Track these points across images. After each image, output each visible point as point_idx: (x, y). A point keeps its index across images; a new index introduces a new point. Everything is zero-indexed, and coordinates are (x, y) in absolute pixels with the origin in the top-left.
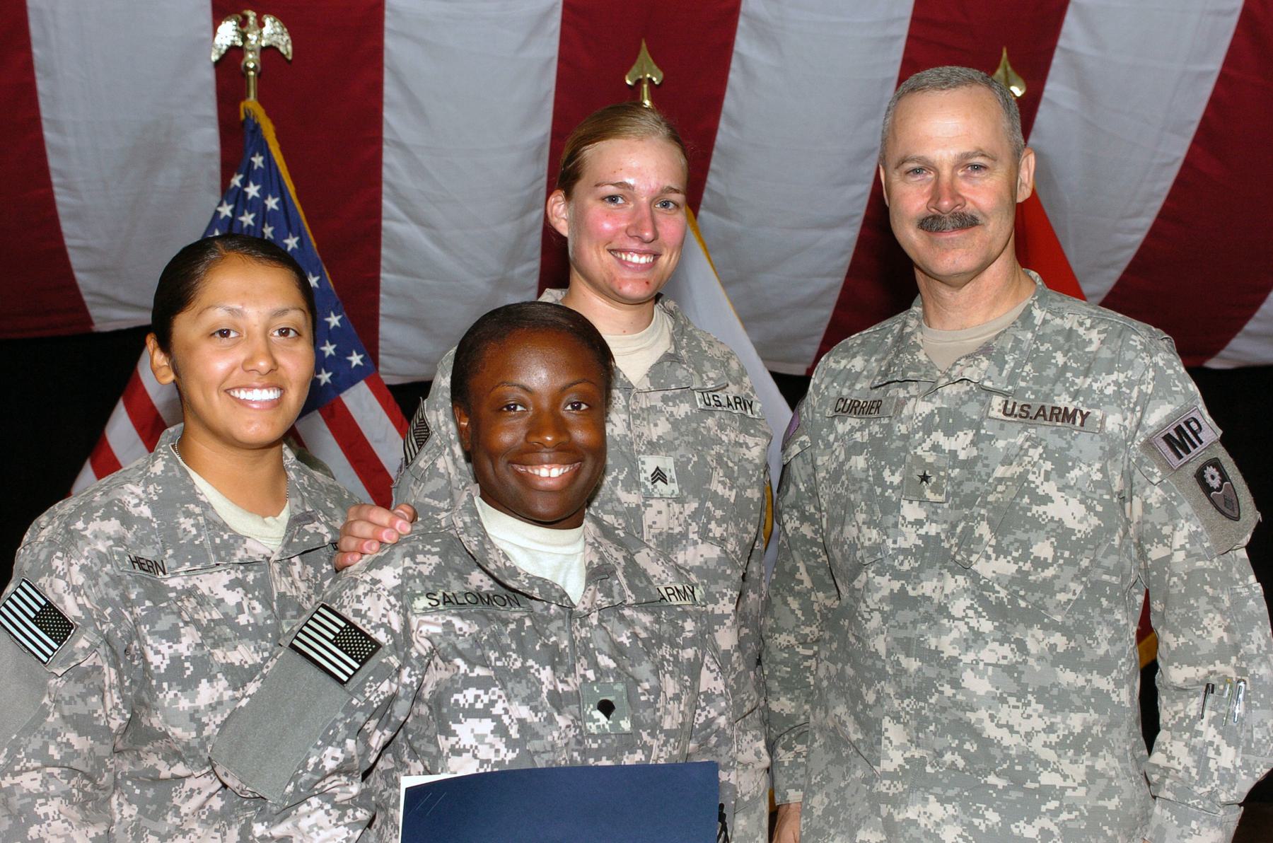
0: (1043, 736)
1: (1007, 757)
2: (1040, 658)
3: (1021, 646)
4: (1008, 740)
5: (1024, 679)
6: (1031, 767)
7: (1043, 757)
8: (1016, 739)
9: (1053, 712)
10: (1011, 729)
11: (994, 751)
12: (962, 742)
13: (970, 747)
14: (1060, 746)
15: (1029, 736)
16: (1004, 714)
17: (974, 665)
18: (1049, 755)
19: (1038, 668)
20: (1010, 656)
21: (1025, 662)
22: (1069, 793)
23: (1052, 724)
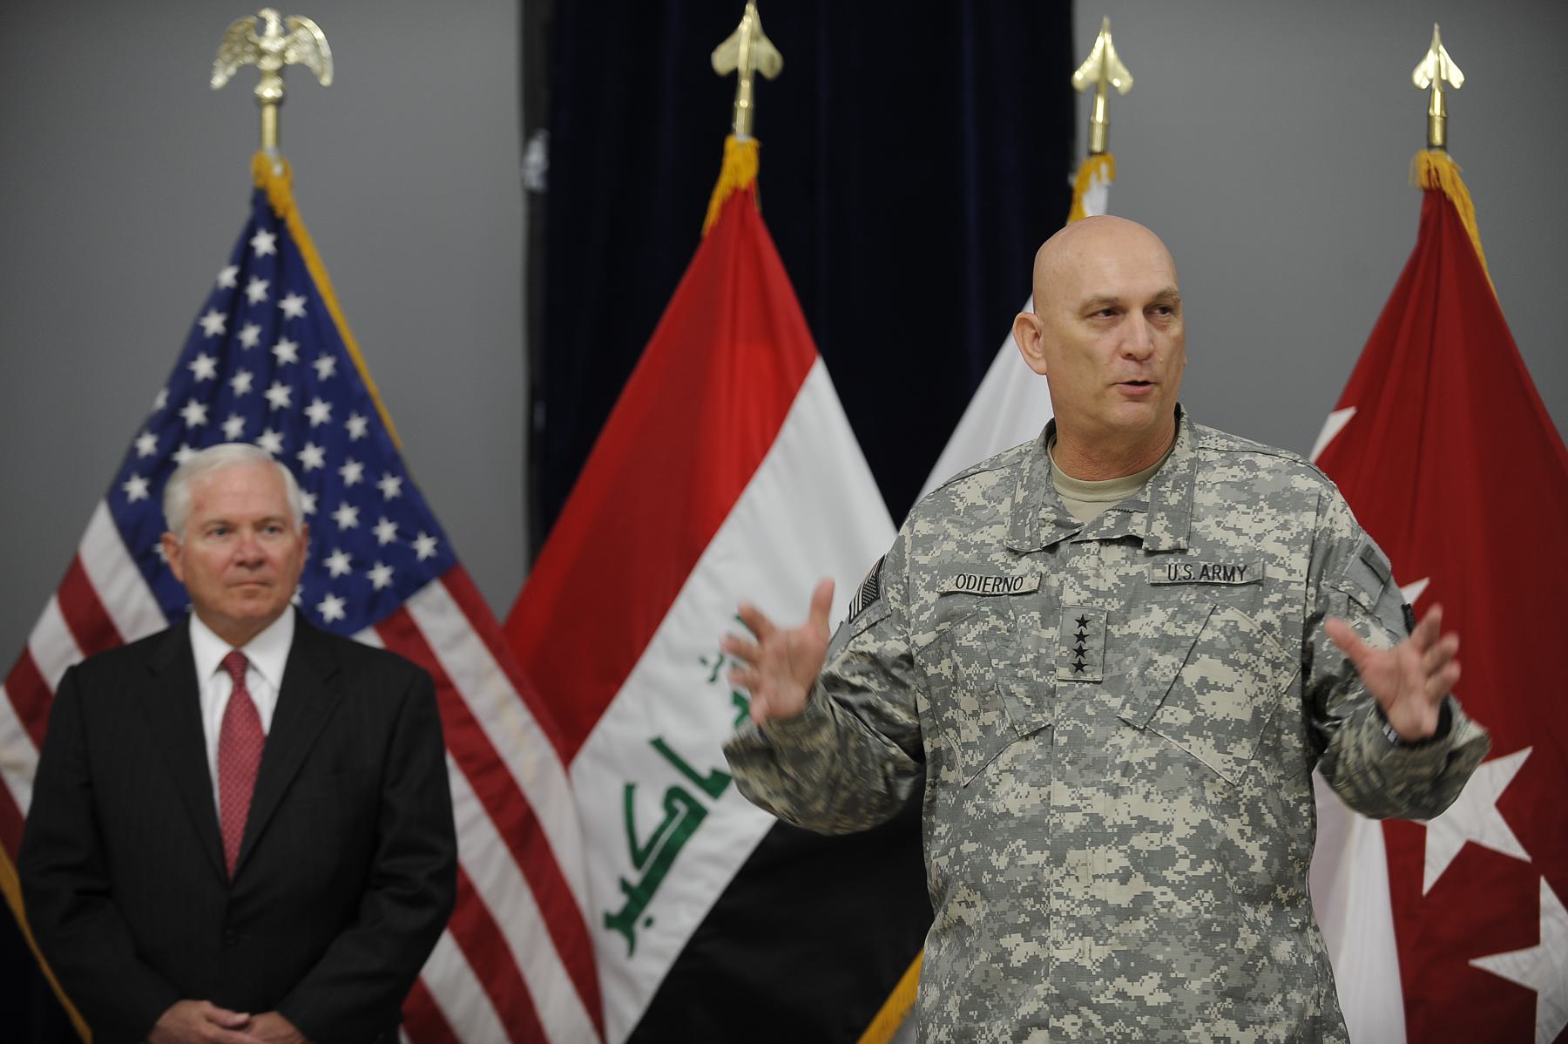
0: (1278, 533)
5: (1255, 489)
8: (1244, 540)
9: (1288, 512)
10: (1239, 532)
15: (1259, 538)
16: (1231, 519)
21: (1256, 477)
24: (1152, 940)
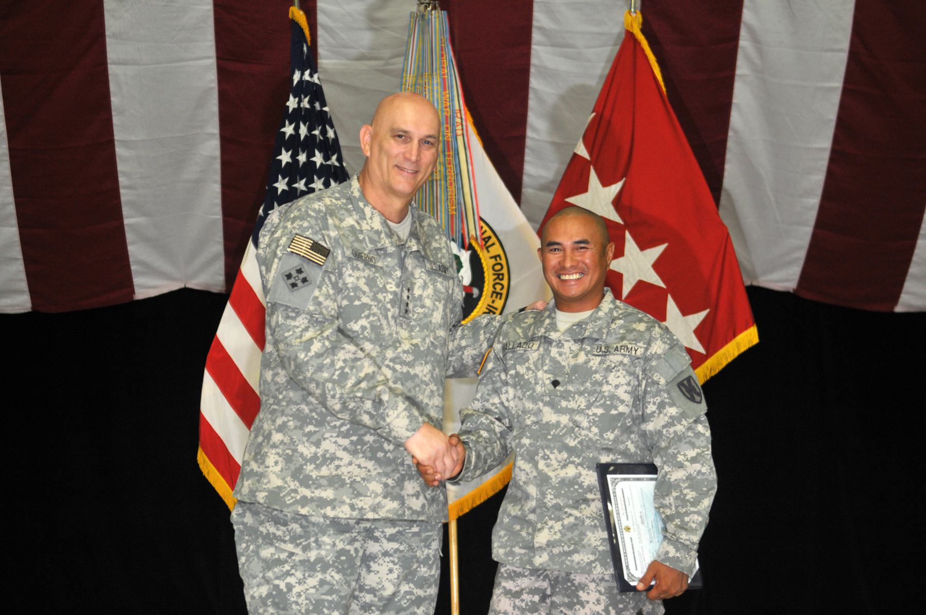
0: (342, 463)
1: (363, 453)
2: (343, 502)
3: (352, 507)
4: (362, 461)
5: (351, 490)
6: (353, 448)
7: (345, 453)
8: (357, 462)
9: (336, 475)
10: (359, 466)
11: (369, 454)
12: (385, 456)
13: (380, 455)
14: (333, 458)
15: (350, 464)
16: (363, 473)
17: (377, 495)
18: (340, 453)
19: (345, 497)
20: (358, 502)
22: (335, 435)
23: (336, 470)
24: (393, 267)
